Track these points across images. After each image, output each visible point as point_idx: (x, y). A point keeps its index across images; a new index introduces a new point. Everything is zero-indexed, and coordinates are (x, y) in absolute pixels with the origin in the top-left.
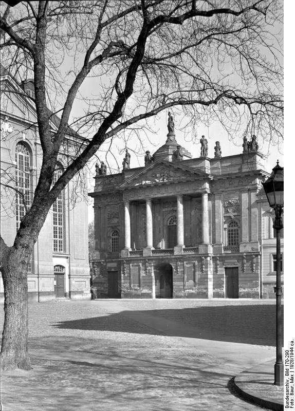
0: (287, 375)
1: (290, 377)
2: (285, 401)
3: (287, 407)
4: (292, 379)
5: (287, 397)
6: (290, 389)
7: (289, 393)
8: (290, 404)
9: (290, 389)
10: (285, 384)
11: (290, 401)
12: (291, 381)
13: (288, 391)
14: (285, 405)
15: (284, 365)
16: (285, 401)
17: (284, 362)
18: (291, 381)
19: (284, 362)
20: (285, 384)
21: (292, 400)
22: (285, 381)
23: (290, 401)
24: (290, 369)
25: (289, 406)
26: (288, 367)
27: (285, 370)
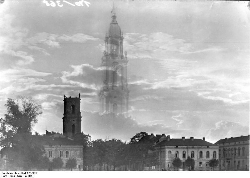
0: (22, 173)
1: (21, 175)
2: (6, 172)
3: (2, 173)
4: (20, 176)
5: (9, 173)
6: (13, 175)
7: (11, 175)
8: (4, 175)
9: (13, 175)
10: (16, 172)
11: (6, 175)
12: (18, 175)
13: (12, 174)
14: (4, 172)
15: (27, 172)
16: (6, 172)
17: (30, 172)
18: (18, 175)
19: (30, 172)
20: (16, 172)
21: (7, 176)
22: (18, 172)
23: (6, 175)
24: (25, 175)
25: (3, 174)
26: (26, 173)
27: (25, 172)
